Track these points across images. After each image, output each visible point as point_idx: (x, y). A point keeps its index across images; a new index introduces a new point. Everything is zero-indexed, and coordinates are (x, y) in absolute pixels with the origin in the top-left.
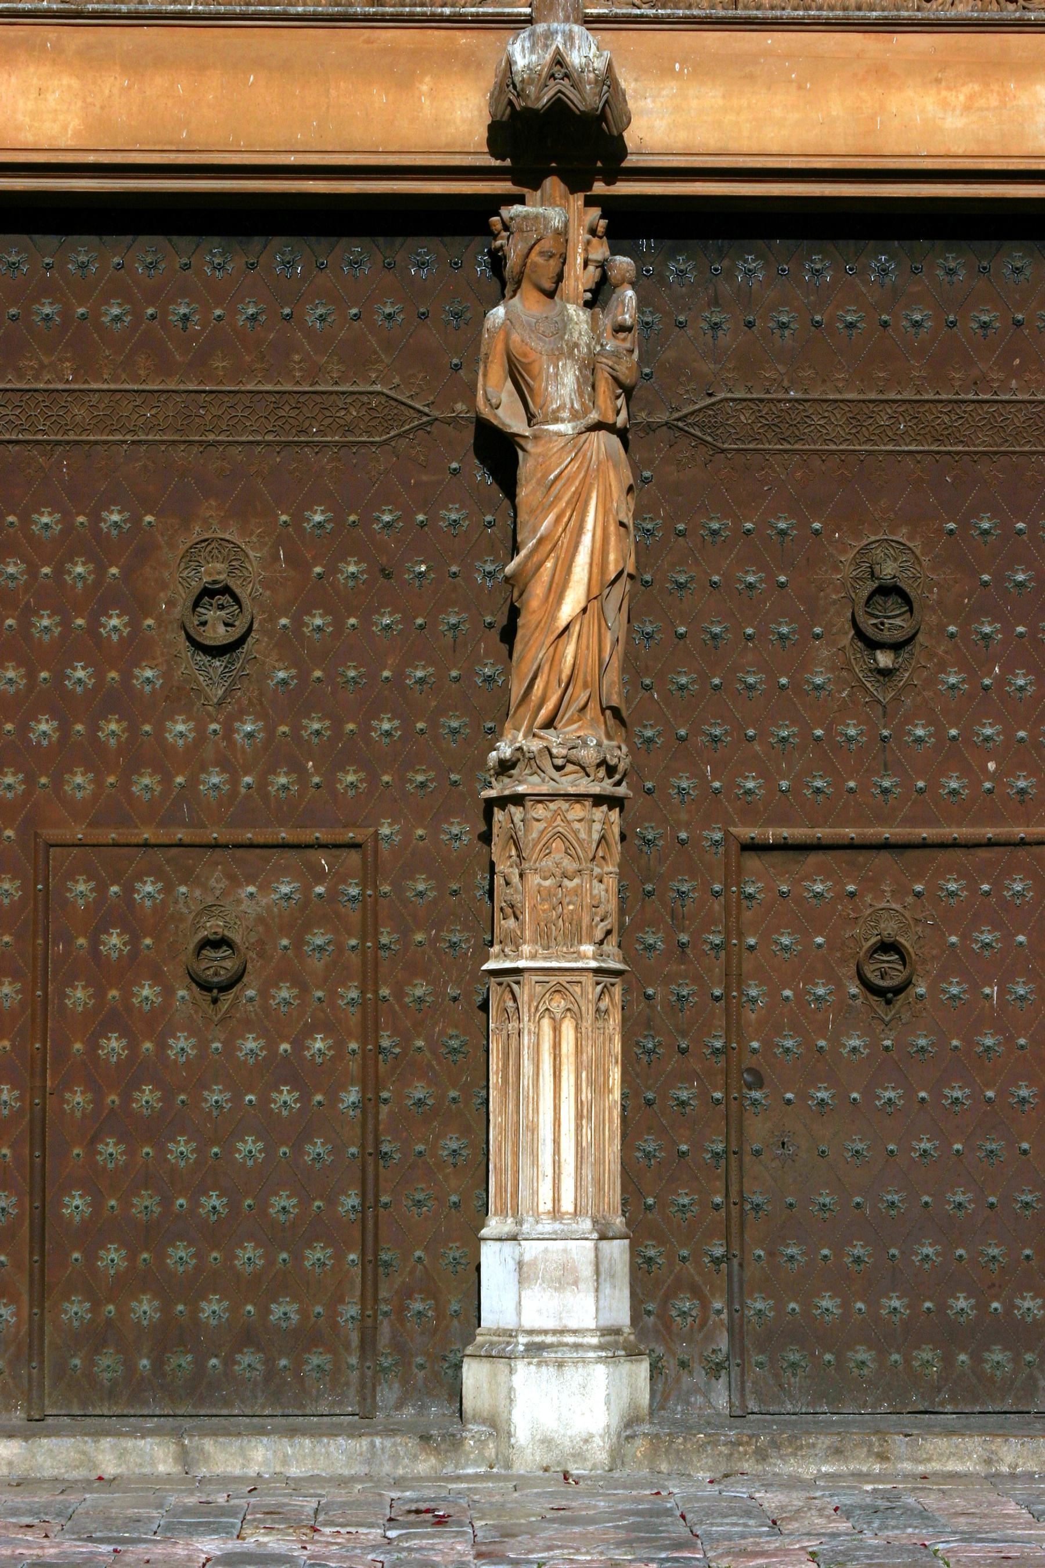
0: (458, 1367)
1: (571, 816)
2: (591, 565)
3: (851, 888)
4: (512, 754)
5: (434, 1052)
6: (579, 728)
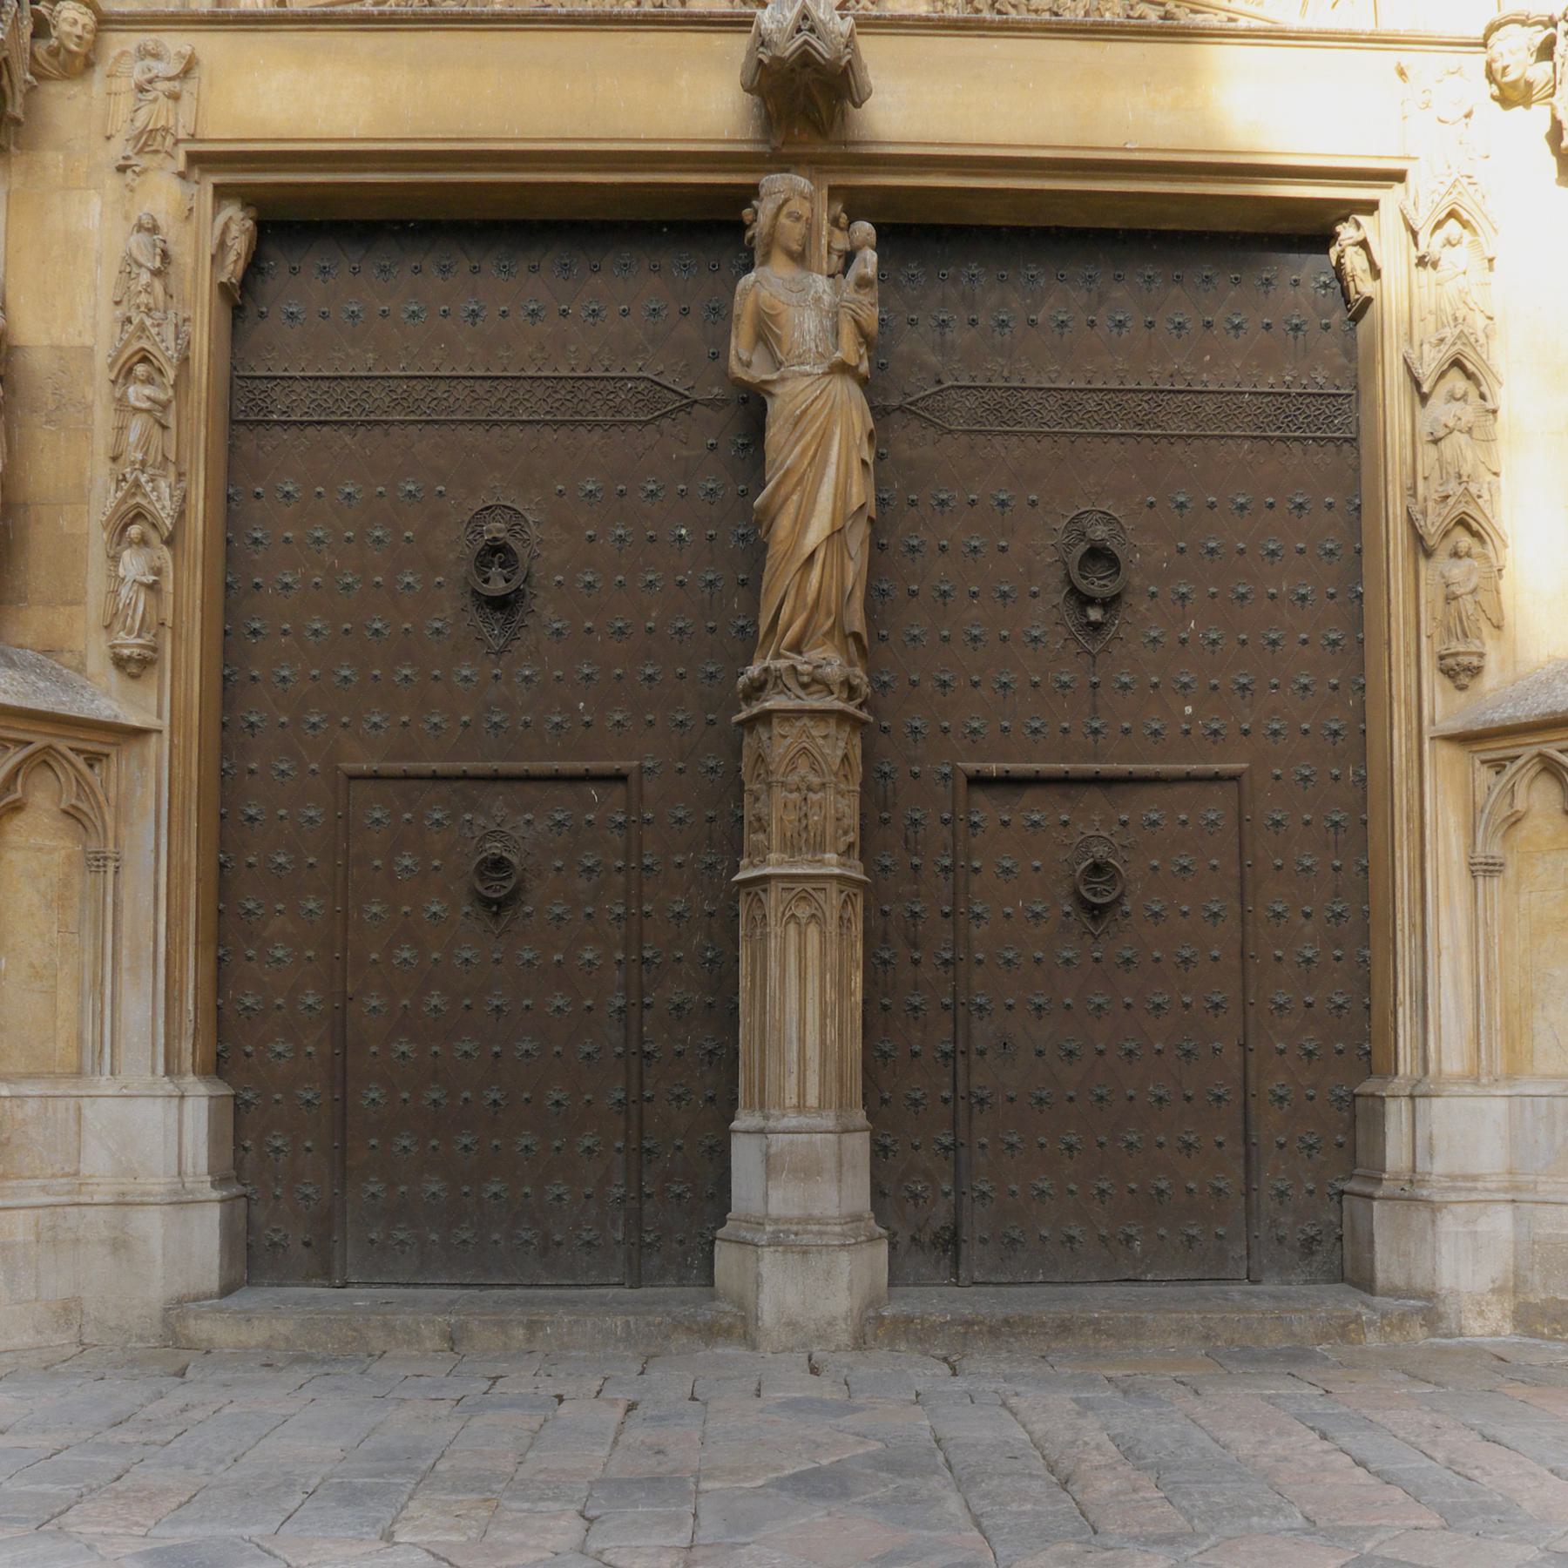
0: (712, 1243)
1: (815, 733)
2: (835, 495)
4: (760, 674)
6: (824, 651)
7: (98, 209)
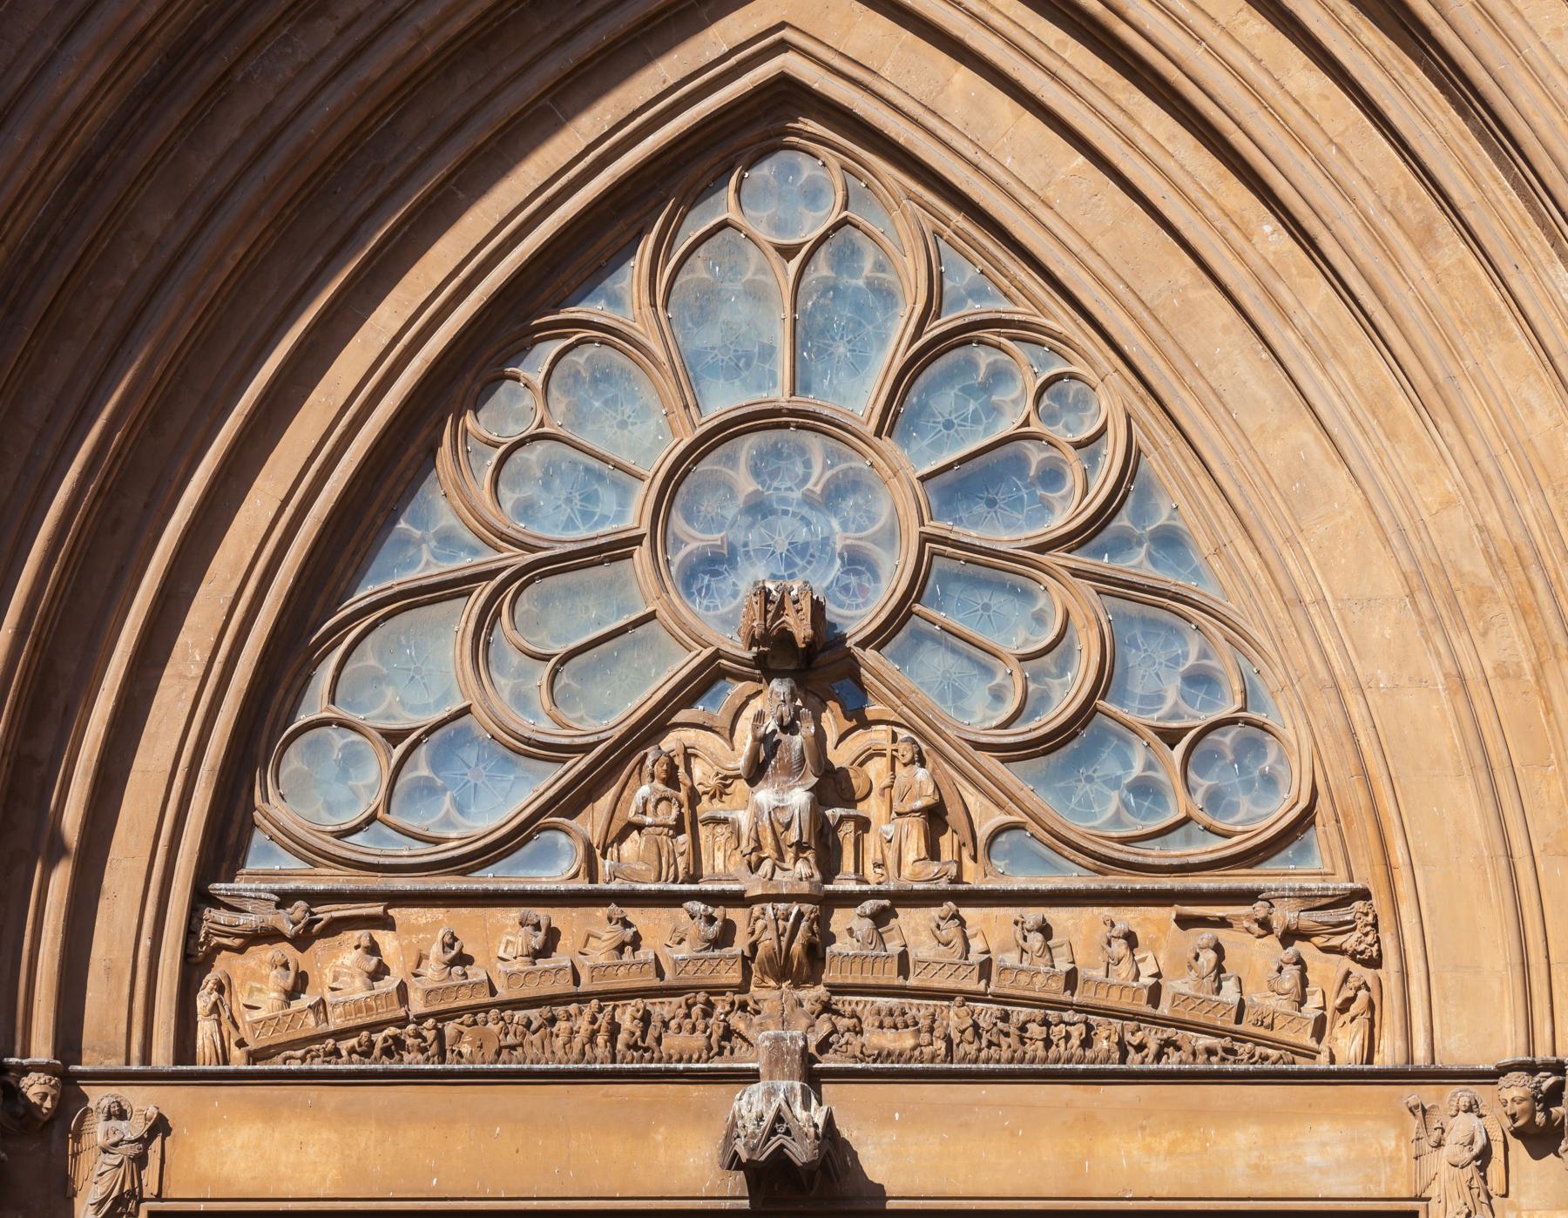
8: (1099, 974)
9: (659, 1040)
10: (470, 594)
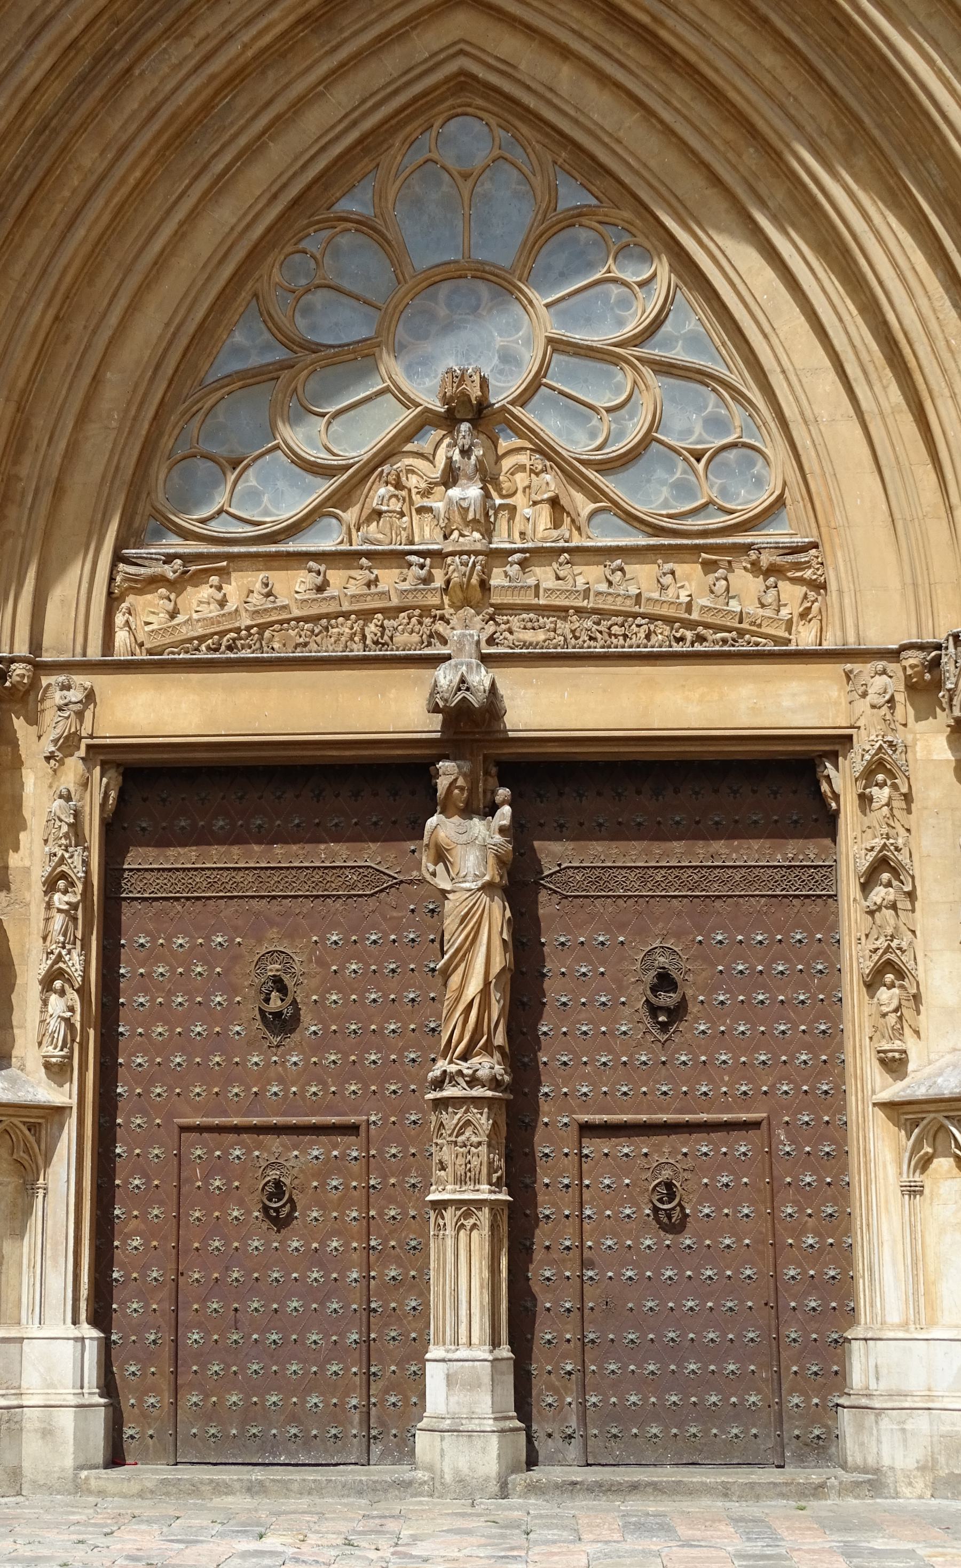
3: (645, 1150)
5: (401, 1248)
7: (32, 781)
8: (655, 595)
9: (391, 638)
10: (278, 378)
